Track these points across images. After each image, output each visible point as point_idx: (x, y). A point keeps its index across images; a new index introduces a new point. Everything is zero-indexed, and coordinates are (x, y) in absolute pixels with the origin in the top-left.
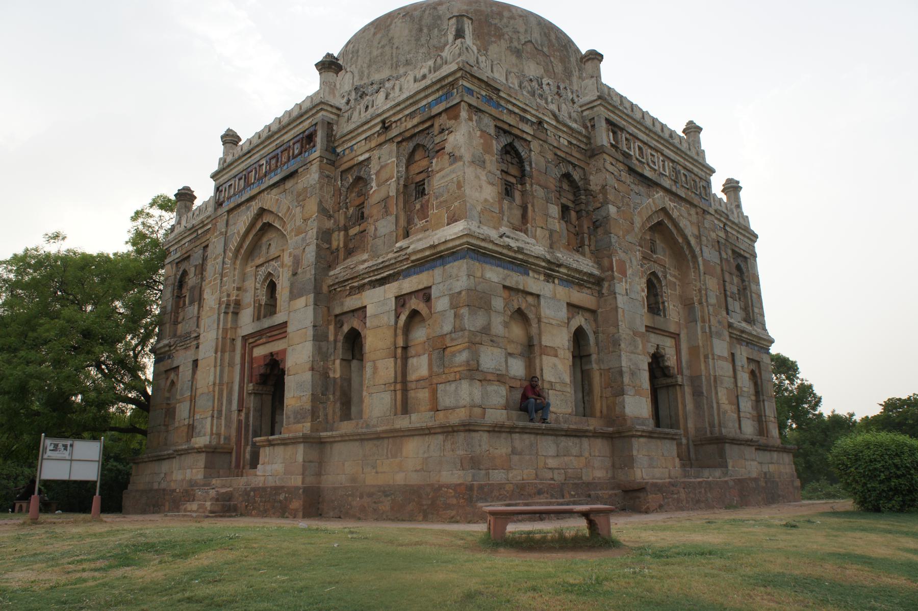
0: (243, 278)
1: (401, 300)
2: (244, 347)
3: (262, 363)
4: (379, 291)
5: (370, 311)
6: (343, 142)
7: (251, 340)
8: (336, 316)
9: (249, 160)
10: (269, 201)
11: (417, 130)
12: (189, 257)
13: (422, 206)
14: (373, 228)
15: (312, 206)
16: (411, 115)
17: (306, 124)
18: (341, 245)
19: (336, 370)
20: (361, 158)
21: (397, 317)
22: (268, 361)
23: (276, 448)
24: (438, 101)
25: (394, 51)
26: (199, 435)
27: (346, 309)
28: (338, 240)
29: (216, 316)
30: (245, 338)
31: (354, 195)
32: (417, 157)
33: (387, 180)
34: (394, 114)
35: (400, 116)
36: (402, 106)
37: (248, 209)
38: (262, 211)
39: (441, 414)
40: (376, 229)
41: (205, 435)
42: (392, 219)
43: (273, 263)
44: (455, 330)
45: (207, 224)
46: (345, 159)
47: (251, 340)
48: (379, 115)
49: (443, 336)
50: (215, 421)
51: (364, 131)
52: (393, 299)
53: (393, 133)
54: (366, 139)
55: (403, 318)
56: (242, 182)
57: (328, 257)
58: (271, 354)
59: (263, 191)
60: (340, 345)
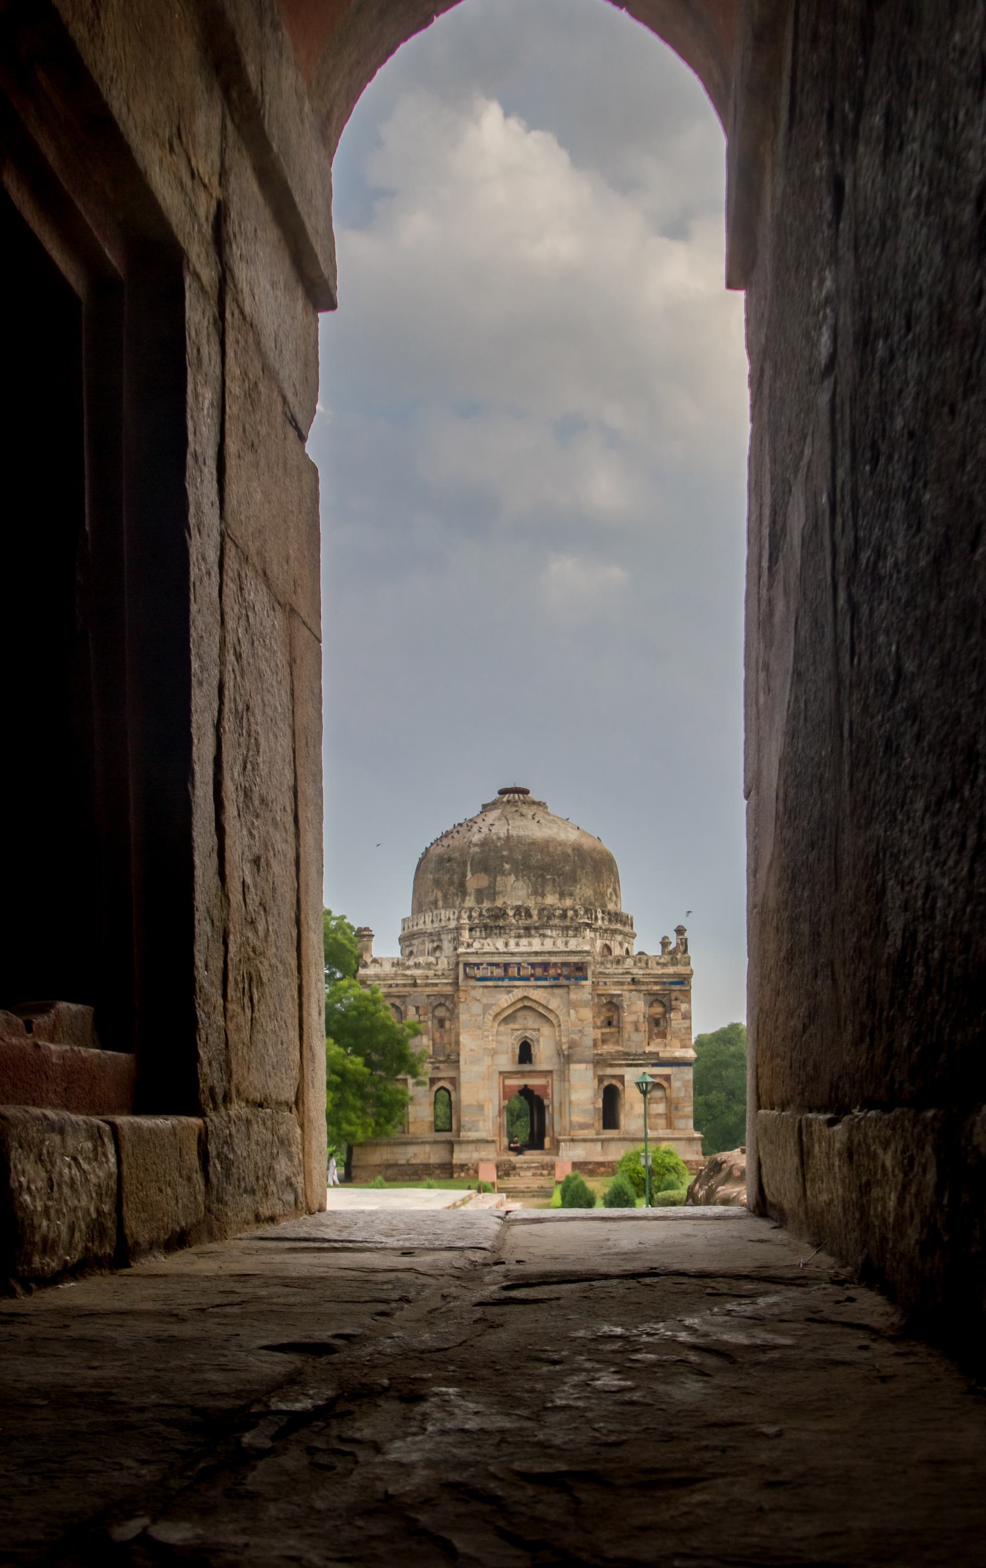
0: (498, 1033)
5: (626, 1079)
10: (537, 995)
12: (405, 996)
13: (659, 1032)
15: (587, 1014)
16: (656, 983)
17: (574, 959)
18: (599, 1036)
19: (600, 1104)
24: (675, 983)
26: (470, 1130)
28: (598, 1034)
30: (500, 1073)
37: (509, 992)
39: (676, 1132)
41: (477, 1131)
42: (642, 1034)
44: (685, 1096)
49: (678, 1098)
57: (595, 1045)
58: (526, 1086)
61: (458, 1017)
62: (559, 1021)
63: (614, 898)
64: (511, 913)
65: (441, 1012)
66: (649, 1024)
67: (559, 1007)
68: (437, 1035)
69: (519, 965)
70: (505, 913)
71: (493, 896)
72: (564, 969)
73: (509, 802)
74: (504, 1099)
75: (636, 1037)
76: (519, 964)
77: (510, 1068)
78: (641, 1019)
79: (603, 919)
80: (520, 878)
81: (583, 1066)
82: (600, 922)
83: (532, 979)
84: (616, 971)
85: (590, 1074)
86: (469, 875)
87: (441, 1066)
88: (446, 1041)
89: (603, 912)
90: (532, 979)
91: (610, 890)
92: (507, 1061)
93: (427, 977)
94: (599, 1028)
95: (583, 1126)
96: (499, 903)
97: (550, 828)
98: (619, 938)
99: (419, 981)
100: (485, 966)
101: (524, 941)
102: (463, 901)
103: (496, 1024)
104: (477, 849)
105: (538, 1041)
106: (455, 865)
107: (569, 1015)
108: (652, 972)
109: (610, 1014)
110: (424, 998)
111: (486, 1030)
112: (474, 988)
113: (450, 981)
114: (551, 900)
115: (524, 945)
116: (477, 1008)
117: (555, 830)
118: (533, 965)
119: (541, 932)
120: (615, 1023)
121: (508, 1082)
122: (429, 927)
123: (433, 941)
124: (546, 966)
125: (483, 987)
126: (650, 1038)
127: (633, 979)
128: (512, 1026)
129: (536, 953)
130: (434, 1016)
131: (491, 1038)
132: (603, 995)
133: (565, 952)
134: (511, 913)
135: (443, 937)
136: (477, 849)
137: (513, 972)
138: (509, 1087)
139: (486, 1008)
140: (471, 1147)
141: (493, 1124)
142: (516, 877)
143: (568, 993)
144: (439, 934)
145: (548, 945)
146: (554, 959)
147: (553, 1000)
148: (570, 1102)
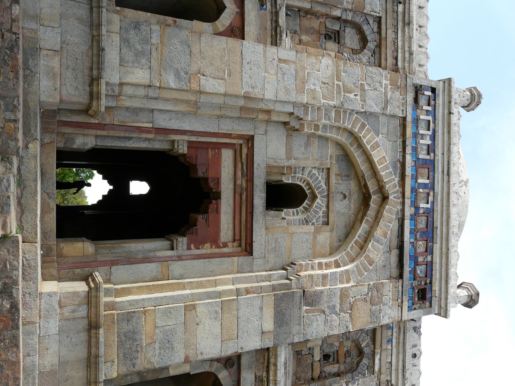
2: (240, 137)
3: (211, 174)
6: (400, 328)
7: (245, 151)
9: (440, 169)
20: (377, 361)
22: (211, 185)
23: (84, 336)
26: (125, 41)
29: (293, 97)
30: (250, 139)
37: (395, 168)
38: (385, 198)
41: (122, 62)
43: (324, 209)
45: (403, 31)
47: (245, 151)
50: (142, 92)
51: (398, 362)
54: (391, 362)
58: (218, 196)
59: (403, 204)
60: (206, 368)
65: (350, 38)
72: (423, 267)
74: (190, 144)
77: (259, 159)
81: (269, 325)
88: (304, 38)
92: (271, 151)
95: (129, 342)
99: (401, 7)
103: (343, 138)
109: (341, 359)
113: (400, 64)
118: (430, 213)
124: (428, 234)
125: (404, 119)
132: (374, 340)
137: (423, 177)
138: (220, 155)
140: (77, 36)
141: (135, 111)
146: (437, 248)
148: (190, 308)
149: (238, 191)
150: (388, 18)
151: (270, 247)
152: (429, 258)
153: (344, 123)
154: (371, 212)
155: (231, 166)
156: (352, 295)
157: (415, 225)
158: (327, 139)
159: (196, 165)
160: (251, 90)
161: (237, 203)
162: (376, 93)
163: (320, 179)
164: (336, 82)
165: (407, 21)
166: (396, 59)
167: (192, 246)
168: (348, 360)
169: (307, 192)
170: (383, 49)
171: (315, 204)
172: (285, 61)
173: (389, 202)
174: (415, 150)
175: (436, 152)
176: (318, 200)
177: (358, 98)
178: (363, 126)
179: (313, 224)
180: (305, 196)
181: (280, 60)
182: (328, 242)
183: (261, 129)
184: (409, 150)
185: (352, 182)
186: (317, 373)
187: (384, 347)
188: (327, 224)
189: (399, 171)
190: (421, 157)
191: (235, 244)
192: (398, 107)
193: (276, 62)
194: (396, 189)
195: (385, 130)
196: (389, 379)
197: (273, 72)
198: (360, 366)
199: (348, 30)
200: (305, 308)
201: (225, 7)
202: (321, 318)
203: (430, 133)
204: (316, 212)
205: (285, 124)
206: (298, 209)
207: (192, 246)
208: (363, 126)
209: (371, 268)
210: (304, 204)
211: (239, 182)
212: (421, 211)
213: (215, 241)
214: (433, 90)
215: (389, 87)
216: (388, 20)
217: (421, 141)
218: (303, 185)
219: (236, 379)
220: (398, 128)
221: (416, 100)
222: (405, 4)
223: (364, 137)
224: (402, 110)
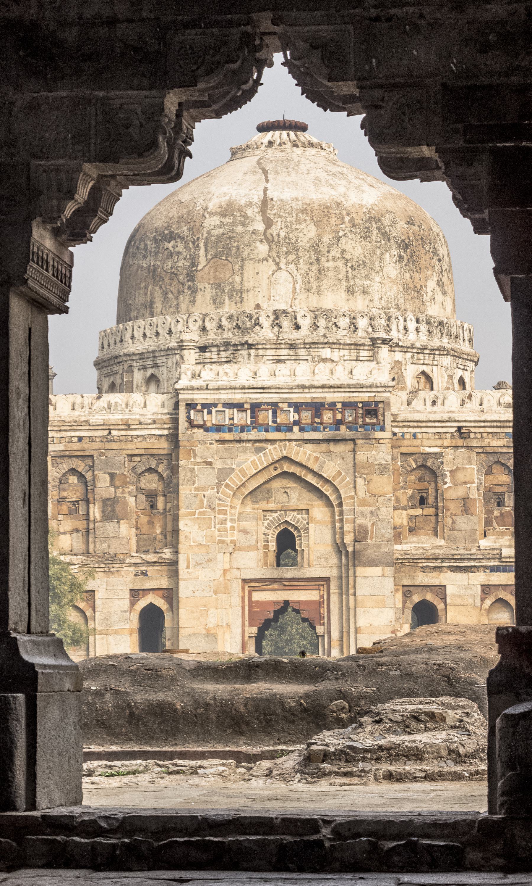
1: (486, 589)
2: (243, 589)
4: (460, 576)
5: (450, 590)
8: (403, 586)
10: (304, 454)
11: (500, 450)
12: (92, 456)
13: (502, 515)
14: (450, 521)
15: (384, 484)
17: (365, 396)
18: (405, 523)
21: (483, 600)
25: (350, 270)
27: (417, 583)
28: (402, 518)
30: (245, 581)
31: (413, 478)
32: (494, 471)
33: (466, 483)
34: (475, 427)
35: (482, 430)
36: (486, 424)
37: (258, 450)
38: (286, 458)
40: (454, 522)
43: (295, 513)
46: (406, 443)
47: (253, 584)
48: (458, 421)
51: (435, 427)
52: (479, 587)
53: (475, 443)
55: (488, 602)
56: (246, 418)
59: (290, 440)
61: (177, 491)
62: (339, 497)
63: (439, 297)
64: (266, 323)
66: (487, 501)
67: (339, 473)
68: (144, 519)
69: (275, 406)
70: (257, 324)
71: (238, 295)
72: (347, 413)
73: (270, 143)
74: (250, 625)
75: (462, 522)
76: (275, 405)
78: (474, 495)
79: (417, 330)
80: (282, 265)
81: (377, 571)
82: (412, 336)
83: (296, 429)
84: (432, 417)
85: (389, 584)
86: (202, 261)
87: (150, 570)
89: (418, 321)
90: (296, 429)
91: (432, 284)
93: (128, 426)
94: (404, 508)
96: (249, 307)
97: (333, 187)
98: (447, 361)
99: (114, 433)
100: (220, 408)
101: (283, 369)
102: (193, 302)
104: (215, 221)
105: (307, 529)
106: (180, 247)
107: (355, 487)
108: (490, 418)
110: (123, 458)
111: (221, 512)
112: (203, 442)
113: (166, 432)
114: (333, 299)
115: (284, 375)
116: (206, 477)
117: (342, 190)
118: (298, 407)
119: (314, 352)
120: (431, 500)
121: (257, 596)
122: (139, 346)
123: (144, 368)
124: (317, 408)
125: (217, 441)
126: (488, 523)
127: (459, 428)
128: (264, 505)
129: (303, 387)
130: (139, 490)
131: (229, 524)
133: (349, 386)
134: (266, 323)
135: (160, 361)
136: (215, 221)
138: (257, 602)
139: (223, 474)
142: (277, 264)
143: (354, 451)
144: (154, 354)
145: (323, 375)
146: (330, 397)
147: (332, 465)
149: (282, 587)
150: (126, 447)
151: (324, 563)
152: (339, 406)
153: (227, 506)
154: (298, 471)
155: (264, 592)
156: (364, 496)
157: (309, 424)
158: (240, 514)
159: (266, 620)
160: (212, 591)
161: (292, 588)
162: (200, 475)
163: (271, 518)
164: (196, 516)
165: (126, 427)
166: (161, 436)
167: (322, 622)
168: (427, 478)
169: (282, 528)
170: (155, 452)
171: (291, 522)
172: (188, 563)
173: (289, 456)
174: (243, 429)
175: (243, 401)
176: (289, 520)
177: (205, 493)
178: (227, 486)
179: (308, 523)
180: (286, 530)
181: (188, 567)
182: (322, 509)
183: (235, 572)
184: (244, 436)
185: (273, 487)
186: (431, 511)
187: (418, 442)
188: (307, 510)
189: (262, 445)
190: (249, 422)
191: (322, 589)
192: (208, 449)
193: (190, 570)
194: (278, 448)
195: (228, 461)
196: (449, 435)
197: (197, 573)
198: (434, 468)
199: (143, 487)
200: (369, 541)
201: (151, 603)
202: (380, 524)
203: (227, 410)
204: (298, 520)
205: (231, 553)
206: (296, 535)
207: (322, 622)
208: (227, 486)
209: (343, 474)
210: (292, 530)
211: (276, 587)
212: (297, 417)
213: (320, 604)
214: (188, 405)
215: (192, 460)
216: (129, 447)
217: (236, 421)
218: (277, 532)
219: (421, 588)
220: (226, 445)
221: (199, 426)
222: (110, 429)
223: (237, 485)
224: (211, 444)
